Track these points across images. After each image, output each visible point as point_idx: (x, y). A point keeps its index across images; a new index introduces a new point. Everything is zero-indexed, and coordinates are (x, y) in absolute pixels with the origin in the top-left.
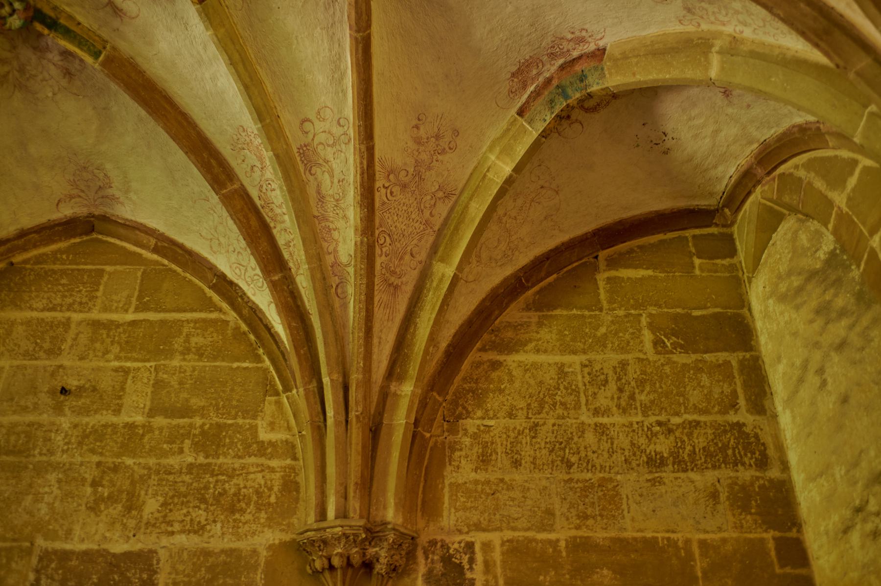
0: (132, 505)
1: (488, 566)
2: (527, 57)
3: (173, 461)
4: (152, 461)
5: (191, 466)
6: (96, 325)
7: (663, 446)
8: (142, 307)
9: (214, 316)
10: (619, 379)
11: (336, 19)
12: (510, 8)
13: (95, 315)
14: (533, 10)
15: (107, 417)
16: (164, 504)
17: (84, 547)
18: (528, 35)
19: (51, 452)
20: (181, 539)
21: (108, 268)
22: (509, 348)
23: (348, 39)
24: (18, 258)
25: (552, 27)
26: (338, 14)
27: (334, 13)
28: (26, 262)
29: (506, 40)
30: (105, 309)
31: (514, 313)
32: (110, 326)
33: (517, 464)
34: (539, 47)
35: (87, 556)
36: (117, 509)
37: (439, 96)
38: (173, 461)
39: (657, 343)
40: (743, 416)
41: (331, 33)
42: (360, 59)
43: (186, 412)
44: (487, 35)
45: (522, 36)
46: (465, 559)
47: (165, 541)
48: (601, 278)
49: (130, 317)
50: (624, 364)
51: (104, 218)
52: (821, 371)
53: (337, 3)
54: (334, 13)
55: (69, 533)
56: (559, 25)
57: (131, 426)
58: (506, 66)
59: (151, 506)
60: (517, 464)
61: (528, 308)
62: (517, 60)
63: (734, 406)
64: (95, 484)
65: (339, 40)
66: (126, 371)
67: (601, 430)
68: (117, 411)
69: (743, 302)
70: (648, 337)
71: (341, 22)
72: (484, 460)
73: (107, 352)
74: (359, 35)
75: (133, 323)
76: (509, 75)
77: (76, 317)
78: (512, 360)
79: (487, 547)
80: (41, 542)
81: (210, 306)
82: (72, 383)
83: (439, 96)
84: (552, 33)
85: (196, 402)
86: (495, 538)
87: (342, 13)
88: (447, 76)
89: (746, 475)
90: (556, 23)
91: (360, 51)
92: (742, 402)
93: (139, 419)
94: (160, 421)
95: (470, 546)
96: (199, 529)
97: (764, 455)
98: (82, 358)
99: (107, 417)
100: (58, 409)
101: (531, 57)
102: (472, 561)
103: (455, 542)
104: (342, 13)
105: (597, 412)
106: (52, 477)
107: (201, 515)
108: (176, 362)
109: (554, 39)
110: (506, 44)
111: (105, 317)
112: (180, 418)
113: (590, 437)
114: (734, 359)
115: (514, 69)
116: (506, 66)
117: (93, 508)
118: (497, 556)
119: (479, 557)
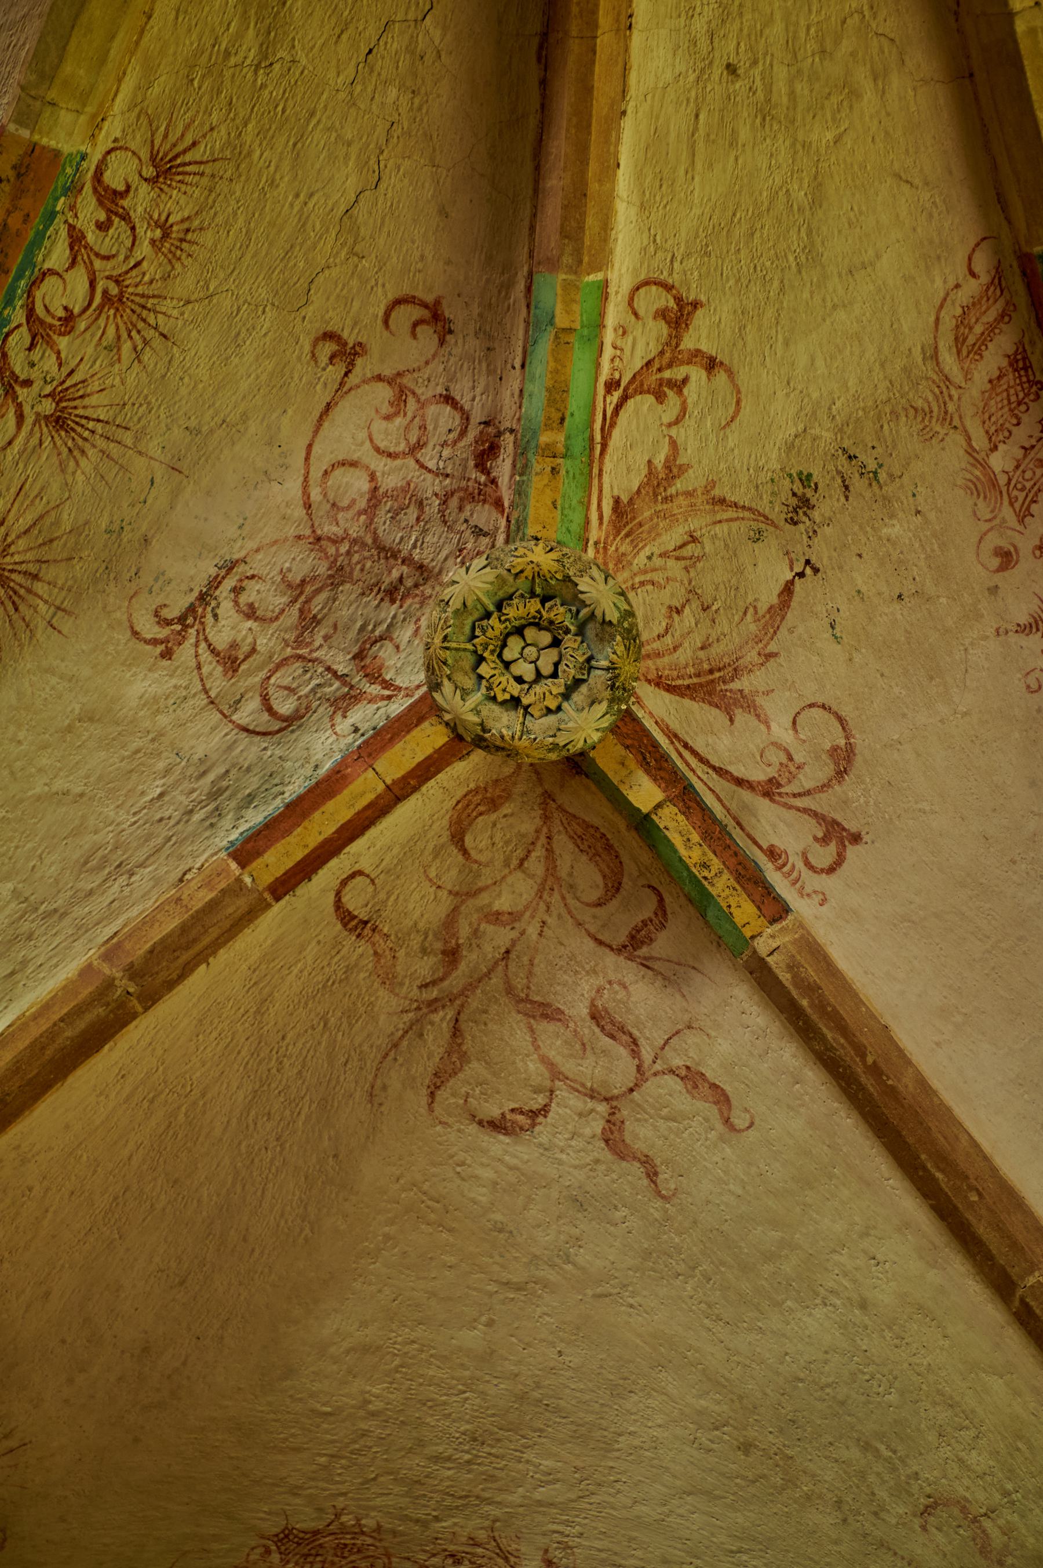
2: (369, 1523)
11: (78, 911)
12: (473, 1338)
14: (522, 1397)
18: (436, 1459)
23: (69, 970)
25: (514, 1498)
26: (98, 904)
27: (91, 893)
29: (373, 1414)
34: (425, 1524)
37: (70, 1381)
41: (25, 927)
42: (60, 1041)
44: (348, 1352)
45: (421, 1443)
53: (123, 880)
54: (91, 893)
56: (540, 1503)
58: (294, 1491)
62: (340, 1502)
65: (25, 963)
71: (82, 929)
74: (124, 984)
76: (273, 1526)
83: (70, 1381)
84: (495, 1512)
87: (110, 913)
88: (146, 1350)
90: (541, 1494)
91: (81, 1025)
101: (379, 1528)
104: (110, 913)
109: (482, 1535)
110: (364, 1426)
112: (590, 133)
115: (306, 1521)
116: (294, 1491)
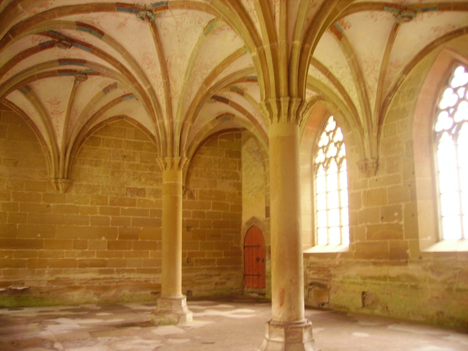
0: (140, 180)
1: (197, 194)
3: (146, 172)
4: (142, 172)
5: (149, 174)
6: (127, 142)
7: (224, 175)
8: (136, 138)
9: (149, 142)
10: (219, 162)
13: (127, 139)
15: (132, 162)
16: (146, 180)
17: (133, 187)
19: (124, 168)
20: (149, 187)
21: (127, 128)
22: (202, 154)
24: (108, 124)
28: (110, 124)
30: (128, 138)
31: (203, 147)
32: (130, 142)
33: (202, 176)
35: (134, 188)
36: (138, 180)
38: (146, 172)
39: (226, 155)
40: (237, 171)
43: (147, 162)
46: (194, 192)
47: (146, 187)
48: (218, 140)
49: (134, 140)
50: (220, 159)
51: (126, 117)
52: (251, 168)
55: (130, 184)
57: (137, 165)
59: (143, 180)
60: (202, 176)
61: (205, 146)
63: (236, 168)
64: (133, 175)
66: (135, 153)
67: (215, 171)
68: (135, 161)
69: (240, 149)
70: (224, 154)
72: (197, 175)
73: (130, 148)
75: (135, 142)
77: (123, 139)
78: (202, 156)
79: (197, 191)
80: (126, 186)
81: (148, 140)
82: (125, 154)
85: (148, 160)
86: (198, 189)
89: (236, 181)
92: (237, 168)
93: (139, 163)
94: (142, 164)
95: (194, 190)
96: (152, 185)
97: (239, 177)
98: (126, 149)
99: (132, 162)
100: (124, 160)
102: (194, 193)
103: (192, 189)
105: (215, 168)
106: (125, 174)
107: (152, 182)
108: (144, 152)
111: (129, 140)
113: (213, 172)
114: (238, 160)
117: (134, 179)
118: (198, 192)
119: (195, 193)
